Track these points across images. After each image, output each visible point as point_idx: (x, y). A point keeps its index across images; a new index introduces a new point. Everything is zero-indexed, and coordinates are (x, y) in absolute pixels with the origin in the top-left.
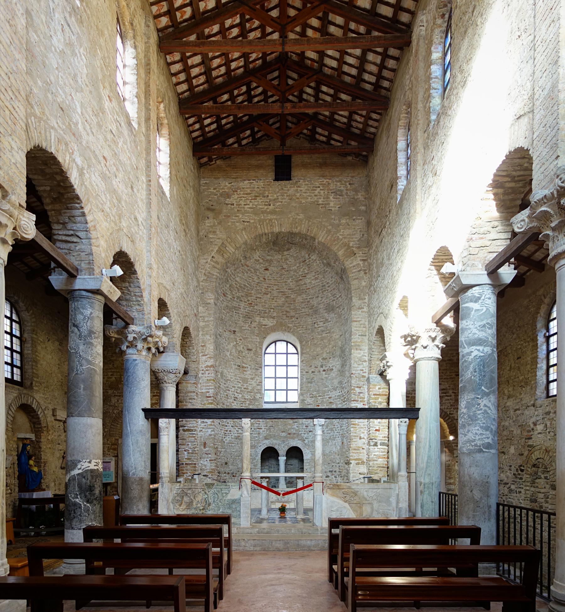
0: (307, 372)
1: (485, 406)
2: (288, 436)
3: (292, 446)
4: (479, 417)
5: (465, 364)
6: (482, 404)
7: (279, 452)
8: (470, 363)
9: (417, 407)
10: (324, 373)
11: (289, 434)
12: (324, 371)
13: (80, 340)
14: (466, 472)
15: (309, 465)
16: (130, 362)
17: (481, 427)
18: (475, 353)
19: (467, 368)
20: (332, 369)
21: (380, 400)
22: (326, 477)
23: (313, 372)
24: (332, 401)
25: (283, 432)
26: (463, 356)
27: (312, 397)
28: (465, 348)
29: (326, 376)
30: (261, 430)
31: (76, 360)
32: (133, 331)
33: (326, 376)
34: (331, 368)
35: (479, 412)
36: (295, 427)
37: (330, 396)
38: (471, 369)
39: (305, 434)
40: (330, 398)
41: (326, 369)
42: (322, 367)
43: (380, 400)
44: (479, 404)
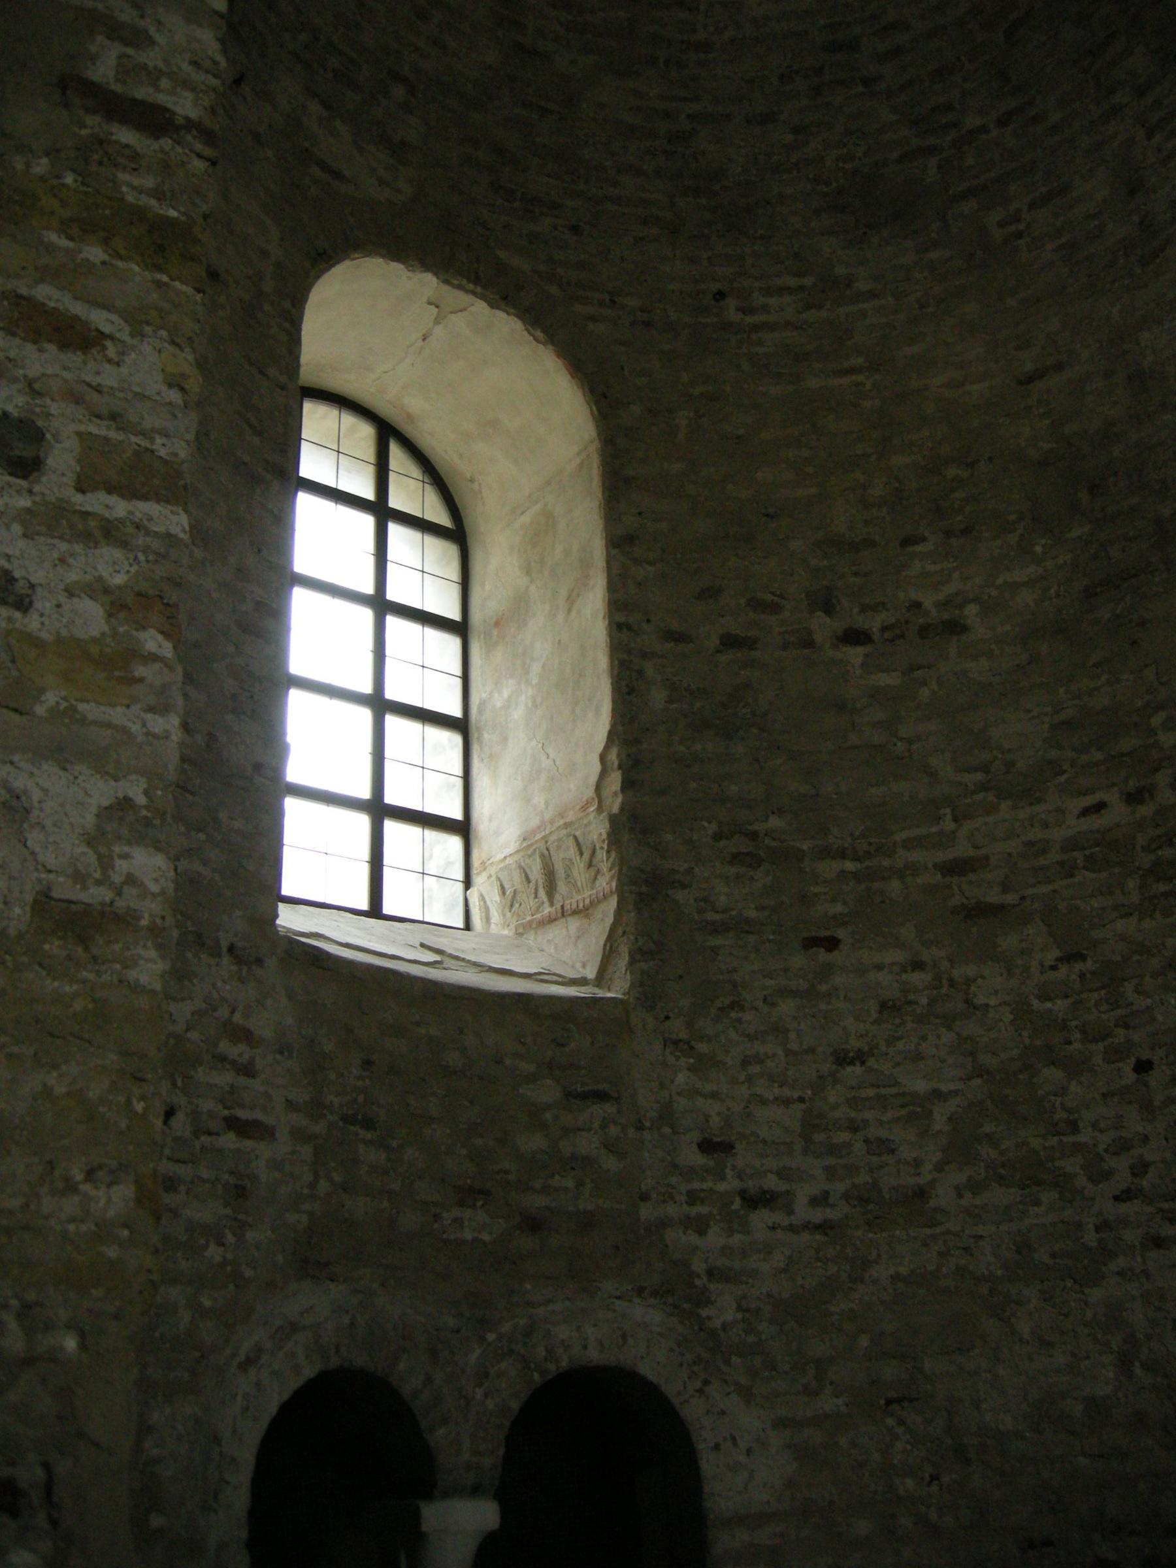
0: (678, 637)
7: (439, 1436)
10: (856, 654)
11: (533, 1224)
23: (730, 642)
24: (993, 897)
25: (468, 1195)
27: (752, 860)
30: (262, 1152)
36: (587, 1144)
37: (963, 850)
39: (700, 1226)
41: (875, 623)
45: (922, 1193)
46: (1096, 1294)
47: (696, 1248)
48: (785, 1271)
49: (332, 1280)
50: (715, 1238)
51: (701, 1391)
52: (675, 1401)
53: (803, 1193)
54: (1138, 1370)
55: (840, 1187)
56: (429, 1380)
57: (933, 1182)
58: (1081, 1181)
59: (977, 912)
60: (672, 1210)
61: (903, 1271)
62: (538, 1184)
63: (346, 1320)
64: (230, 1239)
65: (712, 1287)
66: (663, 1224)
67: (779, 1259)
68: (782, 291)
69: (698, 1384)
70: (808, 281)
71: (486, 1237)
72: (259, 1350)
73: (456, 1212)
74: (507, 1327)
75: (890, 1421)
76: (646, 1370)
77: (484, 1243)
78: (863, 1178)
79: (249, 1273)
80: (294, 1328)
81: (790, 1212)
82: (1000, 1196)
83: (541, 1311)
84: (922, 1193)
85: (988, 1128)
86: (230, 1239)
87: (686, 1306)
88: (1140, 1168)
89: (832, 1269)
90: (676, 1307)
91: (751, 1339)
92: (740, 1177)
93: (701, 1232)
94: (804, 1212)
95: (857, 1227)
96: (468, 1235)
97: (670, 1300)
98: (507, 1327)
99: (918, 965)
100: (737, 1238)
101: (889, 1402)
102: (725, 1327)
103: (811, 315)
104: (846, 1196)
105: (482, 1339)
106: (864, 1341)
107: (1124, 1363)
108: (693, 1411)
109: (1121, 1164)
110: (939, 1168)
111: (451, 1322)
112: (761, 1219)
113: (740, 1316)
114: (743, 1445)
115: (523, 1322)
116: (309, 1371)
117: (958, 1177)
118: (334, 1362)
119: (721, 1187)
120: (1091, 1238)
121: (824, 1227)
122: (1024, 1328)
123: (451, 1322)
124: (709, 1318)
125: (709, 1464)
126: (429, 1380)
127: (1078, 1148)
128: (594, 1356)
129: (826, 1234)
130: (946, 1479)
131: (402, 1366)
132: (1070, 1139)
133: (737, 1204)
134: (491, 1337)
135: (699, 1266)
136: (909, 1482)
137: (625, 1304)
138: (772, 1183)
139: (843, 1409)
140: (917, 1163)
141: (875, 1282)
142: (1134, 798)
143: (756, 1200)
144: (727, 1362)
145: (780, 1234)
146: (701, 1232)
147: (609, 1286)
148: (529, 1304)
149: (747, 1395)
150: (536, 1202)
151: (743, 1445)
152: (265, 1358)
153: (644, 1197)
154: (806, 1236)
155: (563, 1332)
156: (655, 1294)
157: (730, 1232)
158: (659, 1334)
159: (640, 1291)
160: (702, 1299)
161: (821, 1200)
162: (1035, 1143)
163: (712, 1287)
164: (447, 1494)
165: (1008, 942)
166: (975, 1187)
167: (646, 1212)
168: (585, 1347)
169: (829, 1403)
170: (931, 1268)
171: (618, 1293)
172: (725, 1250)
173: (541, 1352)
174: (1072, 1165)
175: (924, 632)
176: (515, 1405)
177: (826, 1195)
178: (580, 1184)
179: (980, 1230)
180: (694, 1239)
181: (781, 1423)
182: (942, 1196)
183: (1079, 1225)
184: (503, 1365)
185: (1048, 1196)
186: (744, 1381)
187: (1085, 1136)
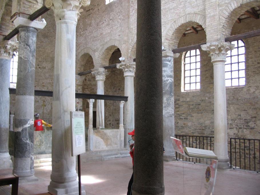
1: (172, 100)
4: (171, 104)
5: (166, 84)
6: (172, 100)
8: (168, 84)
9: (125, 95)
10: (40, 69)
12: (40, 68)
13: (31, 53)
14: (167, 124)
16: (4, 61)
17: (172, 108)
18: (170, 81)
19: (167, 86)
20: (45, 68)
21: (79, 88)
24: (44, 85)
26: (165, 81)
28: (166, 78)
29: (41, 71)
31: (28, 64)
32: (10, 44)
33: (41, 71)
34: (44, 67)
35: (171, 102)
37: (43, 82)
38: (168, 86)
40: (43, 83)
41: (41, 67)
42: (38, 65)
43: (79, 88)
44: (171, 99)
45: (38, 101)
59: (44, 86)
68: (39, 42)
70: (41, 41)
84: (38, 101)
99: (40, 88)
103: (41, 44)
117: (40, 100)
142: (52, 81)
165: (45, 88)
174: (46, 100)
175: (44, 68)
182: (39, 101)
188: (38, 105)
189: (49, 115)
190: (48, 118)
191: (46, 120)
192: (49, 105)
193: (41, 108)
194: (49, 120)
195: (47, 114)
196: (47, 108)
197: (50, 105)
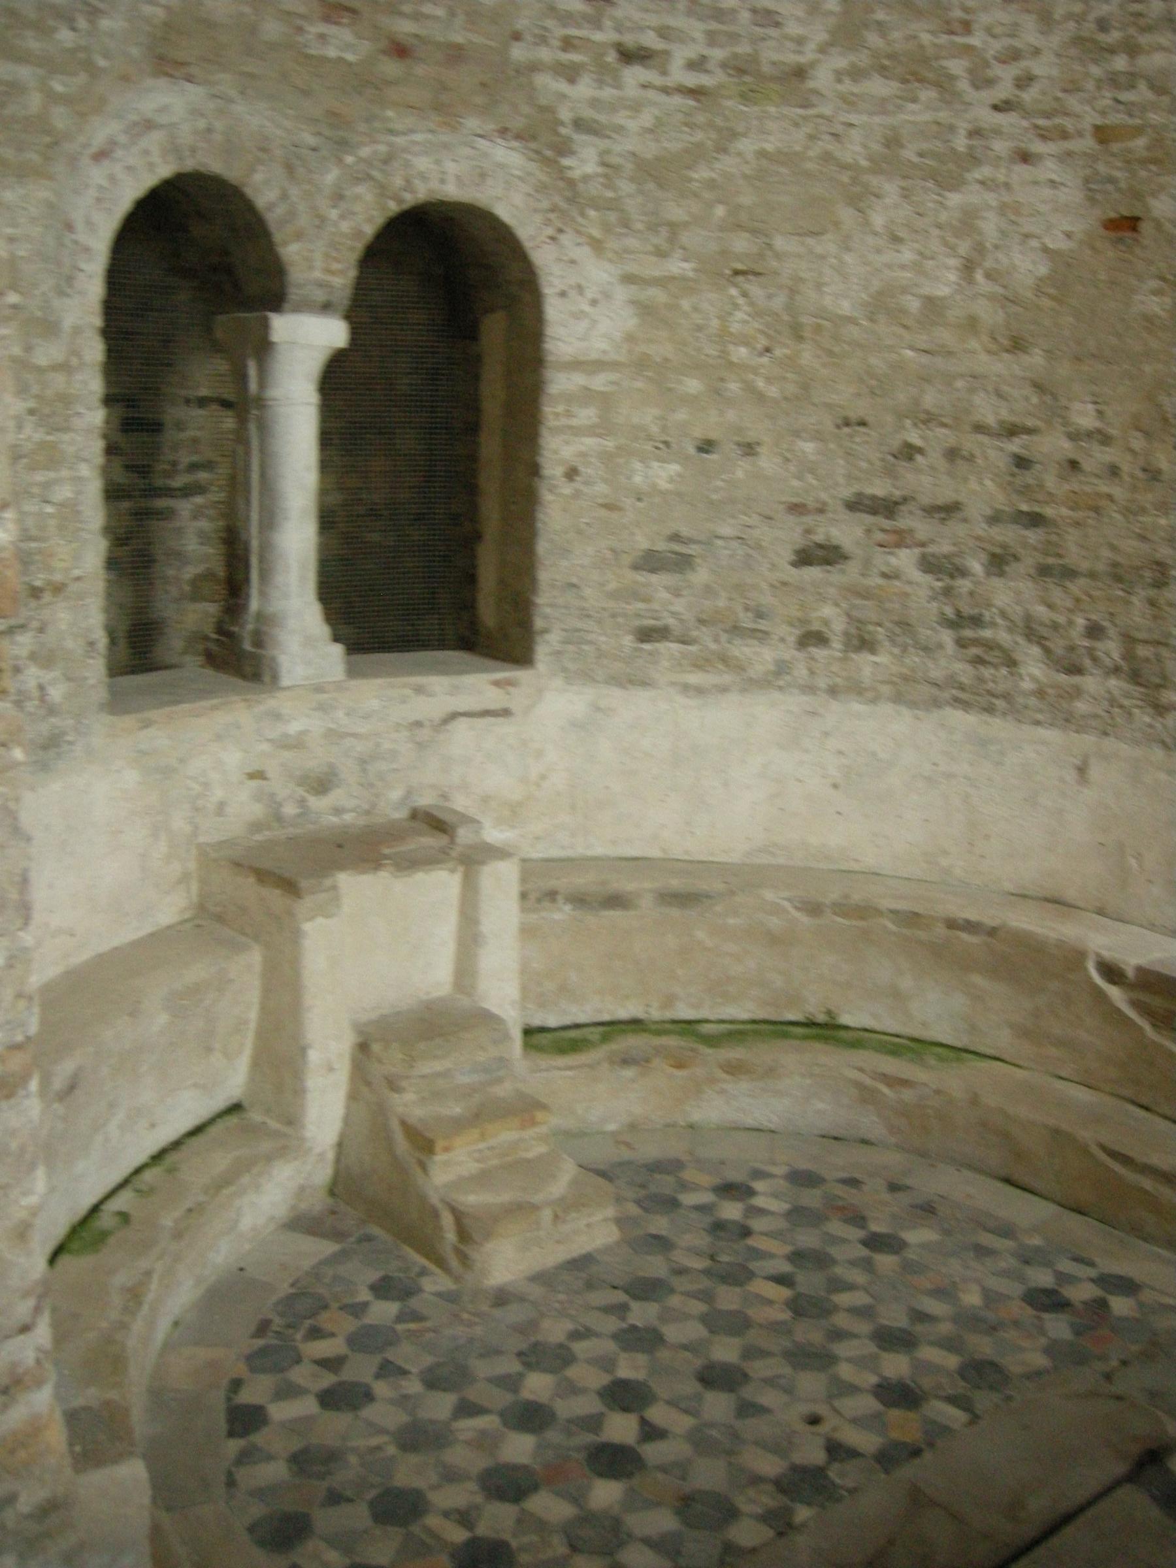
2: (391, 68)
3: (421, 193)
7: (291, 252)
11: (400, 50)
15: (604, 428)
22: (804, 558)
39: (571, 73)
45: (800, 73)
46: (954, 199)
47: (564, 96)
48: (651, 131)
49: (189, 81)
50: (584, 89)
51: (552, 238)
52: (528, 244)
53: (681, 54)
54: (979, 276)
55: (718, 54)
56: (284, 196)
57: (813, 64)
58: (963, 85)
60: (545, 54)
61: (769, 147)
62: (407, 8)
63: (202, 124)
64: (82, 23)
65: (575, 136)
66: (534, 67)
67: (647, 118)
69: (550, 231)
71: (350, 57)
72: (113, 143)
73: (322, 28)
74: (365, 152)
75: (733, 292)
76: (503, 212)
77: (350, 64)
78: (743, 49)
79: (102, 63)
80: (149, 125)
81: (664, 73)
82: (878, 87)
83: (400, 140)
84: (800, 73)
85: (880, 15)
86: (82, 23)
87: (549, 153)
88: (1025, 81)
89: (699, 136)
90: (537, 152)
91: (610, 194)
92: (618, 29)
93: (572, 81)
94: (678, 75)
95: (730, 98)
96: (332, 53)
97: (533, 145)
98: (365, 152)
100: (607, 93)
101: (737, 273)
102: (586, 178)
104: (724, 65)
105: (340, 161)
106: (720, 211)
107: (968, 268)
108: (543, 257)
109: (1006, 74)
110: (823, 50)
111: (311, 140)
112: (634, 75)
113: (600, 170)
114: (590, 294)
115: (382, 148)
116: (165, 171)
117: (839, 61)
118: (189, 165)
119: (598, 37)
120: (961, 143)
121: (695, 93)
122: (878, 220)
123: (311, 140)
124: (570, 168)
125: (554, 310)
126: (284, 196)
127: (968, 49)
128: (452, 191)
129: (698, 101)
130: (778, 352)
131: (258, 177)
132: (959, 39)
133: (611, 57)
134: (349, 159)
135: (565, 114)
136: (743, 351)
137: (487, 143)
138: (650, 40)
139: (691, 274)
140: (800, 41)
141: (739, 154)
143: (630, 56)
144: (583, 215)
145: (651, 94)
146: (572, 81)
147: (472, 123)
148: (391, 132)
149: (597, 246)
150: (405, 28)
151: (590, 294)
152: (119, 153)
153: (517, 37)
154: (677, 100)
155: (423, 163)
156: (518, 137)
157: (601, 83)
158: (520, 178)
159: (503, 132)
160: (564, 148)
161: (698, 65)
162: (926, 38)
163: (575, 136)
164: (298, 309)
166: (856, 74)
167: (518, 53)
168: (443, 181)
169: (677, 266)
170: (798, 148)
171: (479, 132)
172: (594, 103)
173: (398, 182)
174: (957, 66)
176: (370, 230)
177: (704, 59)
178: (452, 14)
179: (853, 118)
180: (562, 86)
181: (629, 279)
182: (822, 79)
183: (952, 128)
184: (361, 189)
185: (928, 94)
186: (596, 233)
187: (975, 41)
188: (784, 158)
189: (1036, 359)
190: (988, 411)
191: (952, 454)
192: (1025, 157)
193: (846, 215)
194: (1015, 446)
195: (972, 324)
196: (990, 226)
197: (1050, 169)
